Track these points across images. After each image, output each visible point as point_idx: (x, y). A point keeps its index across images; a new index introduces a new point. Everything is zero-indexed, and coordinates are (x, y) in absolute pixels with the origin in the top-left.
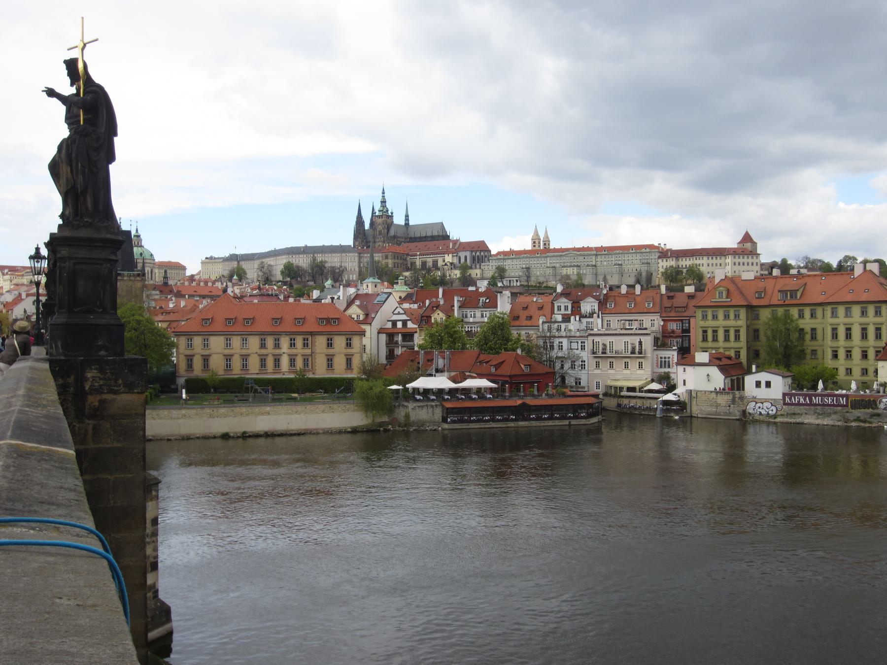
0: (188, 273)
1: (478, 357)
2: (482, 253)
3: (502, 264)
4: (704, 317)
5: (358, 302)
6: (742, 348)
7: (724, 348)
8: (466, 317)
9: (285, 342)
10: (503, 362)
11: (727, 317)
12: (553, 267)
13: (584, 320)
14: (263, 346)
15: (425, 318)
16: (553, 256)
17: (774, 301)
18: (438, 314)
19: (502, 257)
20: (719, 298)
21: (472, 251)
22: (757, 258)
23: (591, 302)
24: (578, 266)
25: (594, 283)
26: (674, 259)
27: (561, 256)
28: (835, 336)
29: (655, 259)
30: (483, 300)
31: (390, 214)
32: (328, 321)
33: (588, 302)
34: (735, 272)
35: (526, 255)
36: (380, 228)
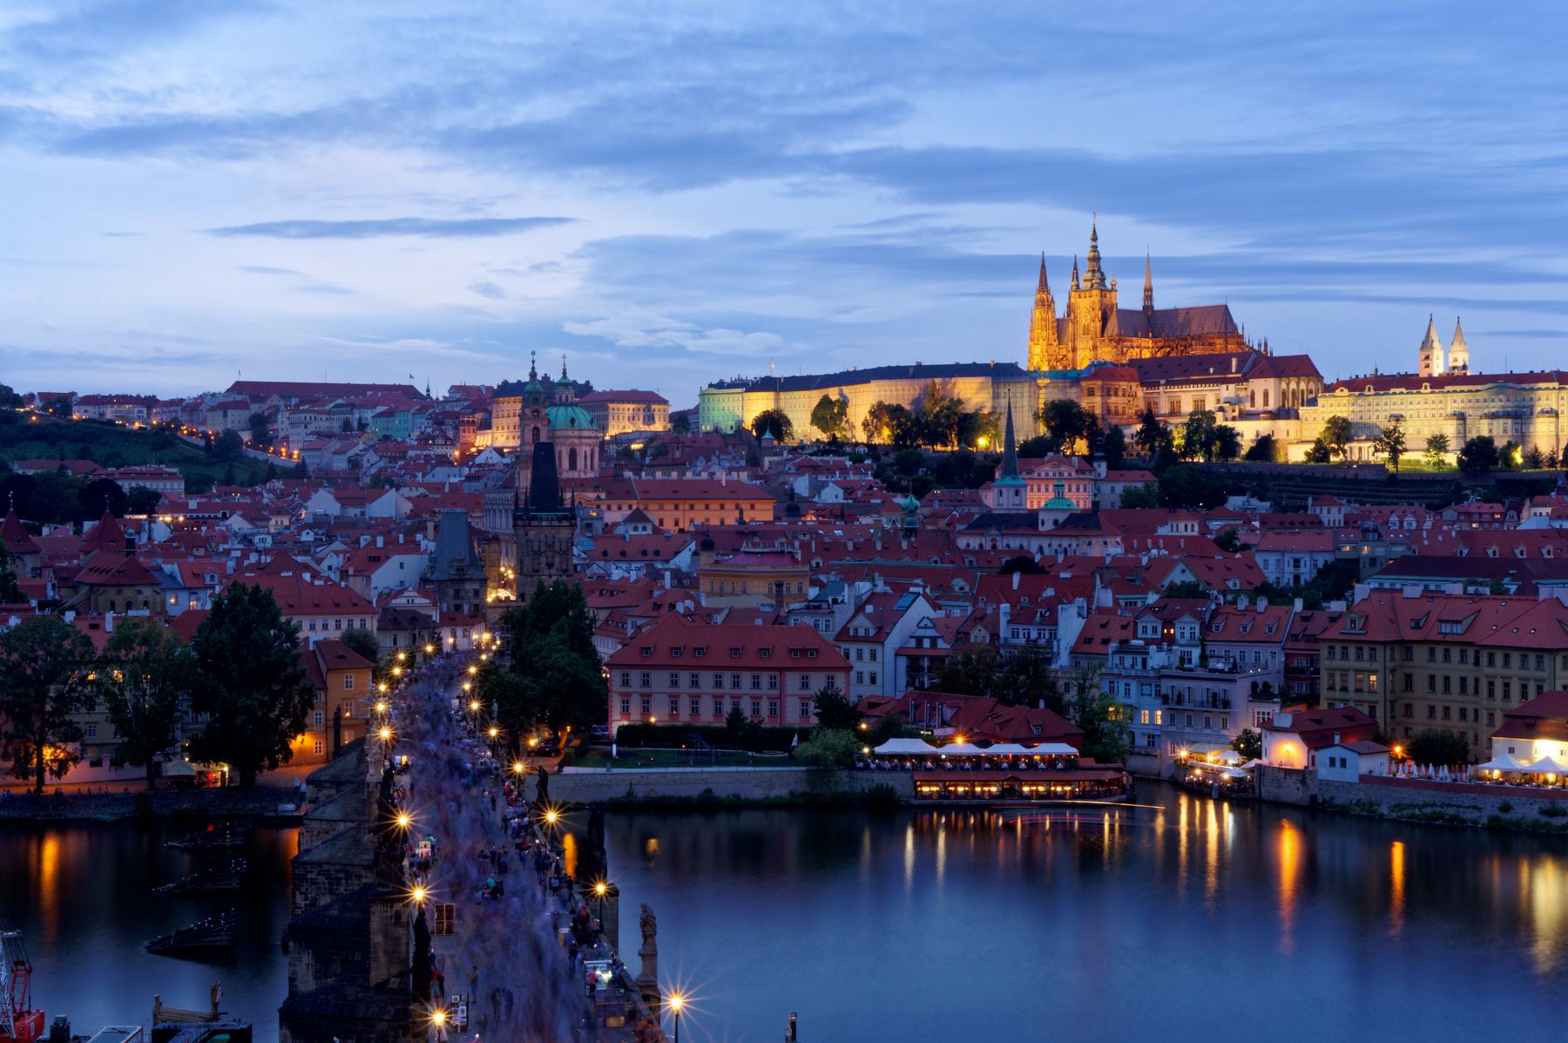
0: (672, 410)
1: (993, 709)
2: (1303, 386)
4: (1331, 655)
5: (869, 609)
6: (1377, 702)
7: (1355, 701)
8: (1018, 637)
9: (746, 679)
10: (1011, 720)
11: (1359, 657)
14: (718, 684)
15: (962, 635)
17: (1433, 636)
20: (1351, 628)
23: (1189, 623)
28: (1491, 694)
32: (804, 652)
35: (1398, 390)
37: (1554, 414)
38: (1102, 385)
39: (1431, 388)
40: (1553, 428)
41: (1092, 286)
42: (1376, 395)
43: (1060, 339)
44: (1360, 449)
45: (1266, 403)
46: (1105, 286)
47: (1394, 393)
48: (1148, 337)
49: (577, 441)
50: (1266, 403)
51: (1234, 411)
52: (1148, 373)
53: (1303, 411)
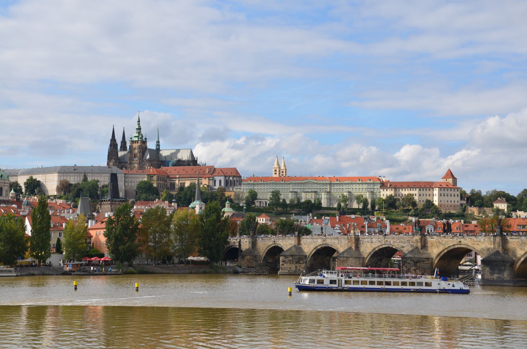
2: (235, 179)
3: (252, 188)
12: (295, 192)
16: (295, 184)
19: (252, 182)
21: (225, 176)
22: (458, 191)
23: (430, 227)
24: (315, 192)
25: (329, 206)
26: (393, 190)
27: (301, 183)
29: (378, 188)
31: (144, 140)
33: (429, 227)
34: (441, 201)
35: (272, 182)
36: (136, 151)
46: (143, 139)
49: (3, 184)
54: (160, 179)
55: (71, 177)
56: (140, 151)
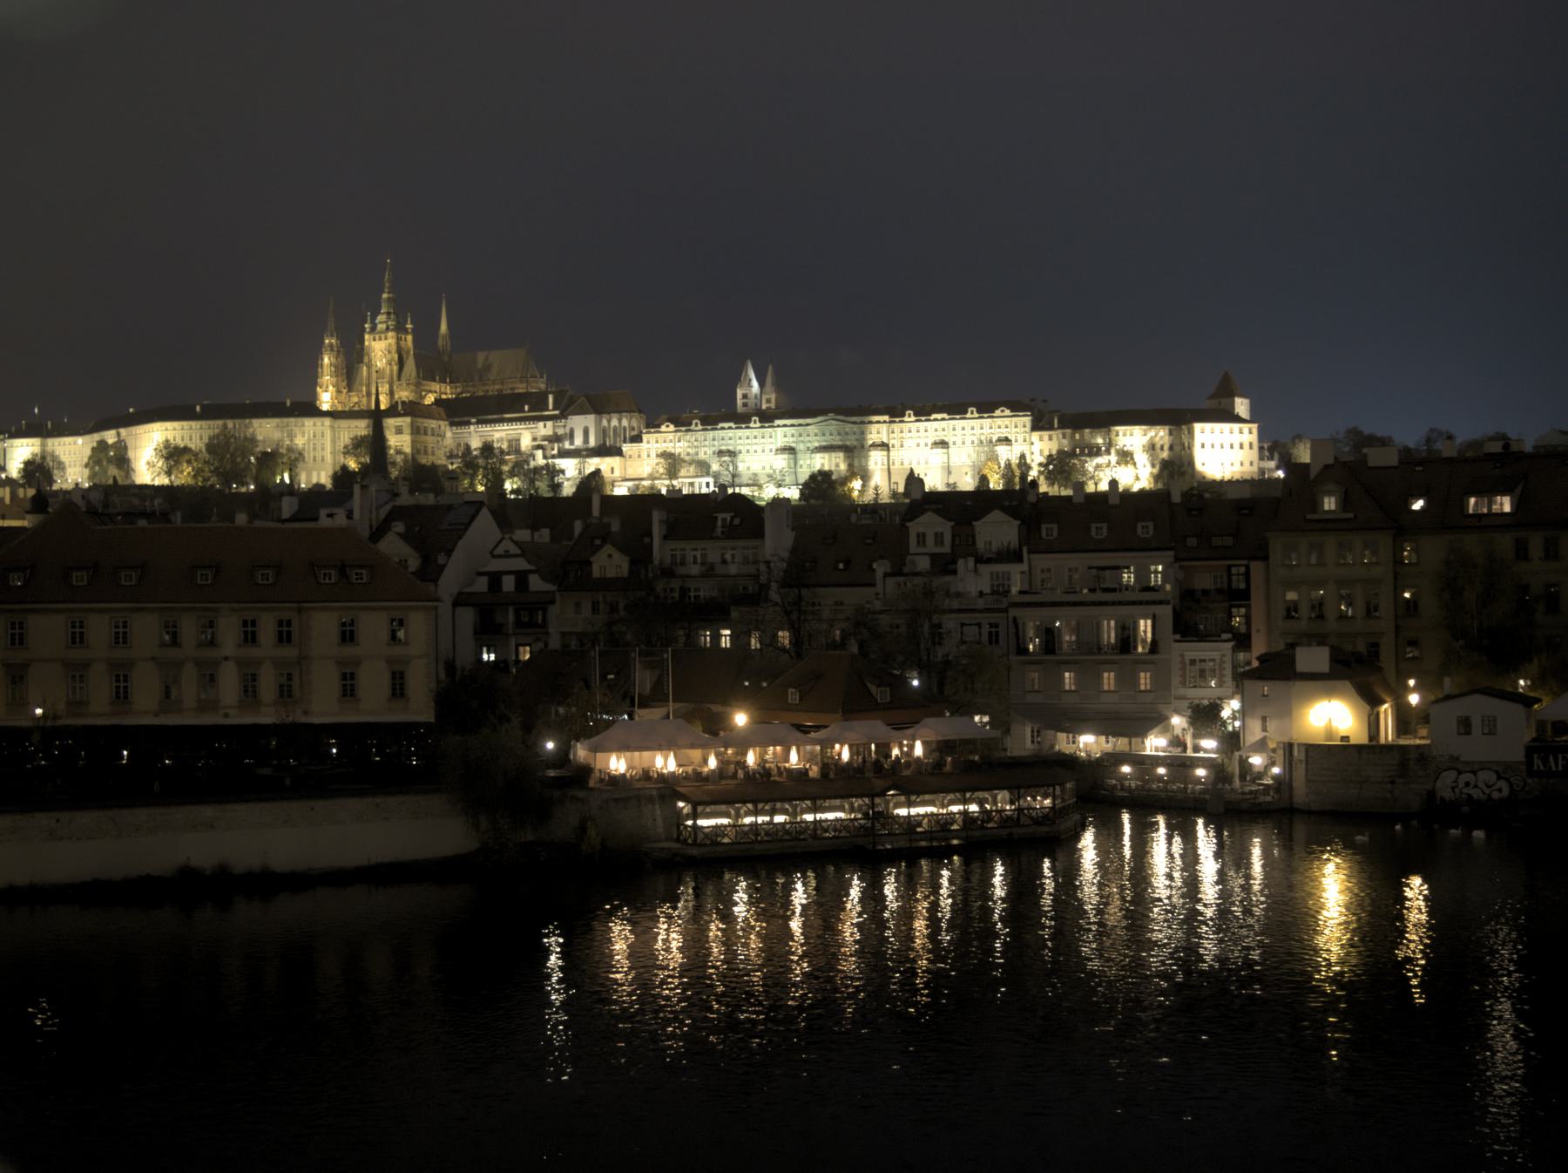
2: (625, 423)
5: (399, 527)
8: (683, 563)
13: (985, 569)
18: (610, 556)
30: (724, 520)
34: (1203, 464)
35: (726, 425)
37: (885, 446)
38: (412, 422)
39: (760, 422)
40: (886, 463)
41: (388, 329)
42: (703, 430)
43: (350, 388)
44: (692, 484)
45: (586, 440)
47: (723, 428)
48: (446, 383)
50: (586, 440)
51: (553, 449)
52: (458, 412)
53: (626, 448)
54: (422, 431)
55: (194, 435)
56: (392, 359)
